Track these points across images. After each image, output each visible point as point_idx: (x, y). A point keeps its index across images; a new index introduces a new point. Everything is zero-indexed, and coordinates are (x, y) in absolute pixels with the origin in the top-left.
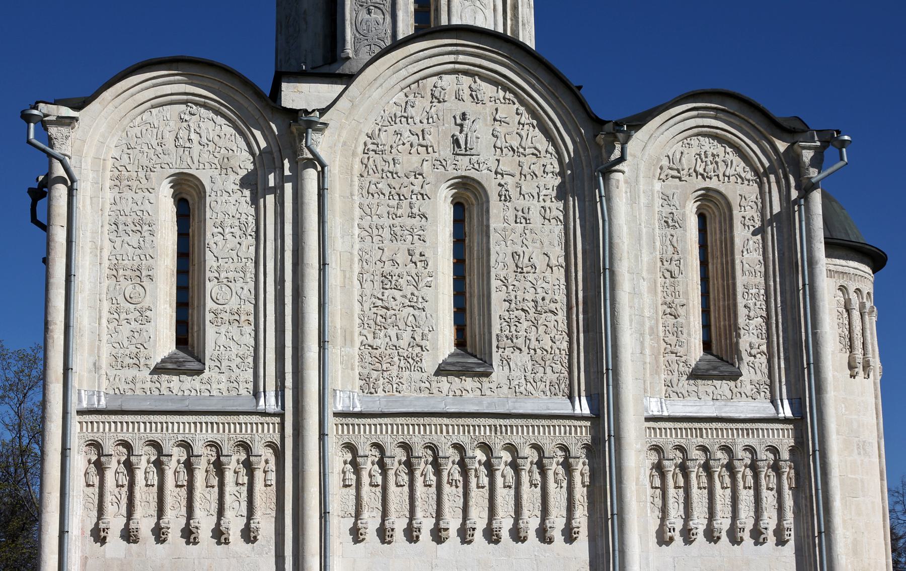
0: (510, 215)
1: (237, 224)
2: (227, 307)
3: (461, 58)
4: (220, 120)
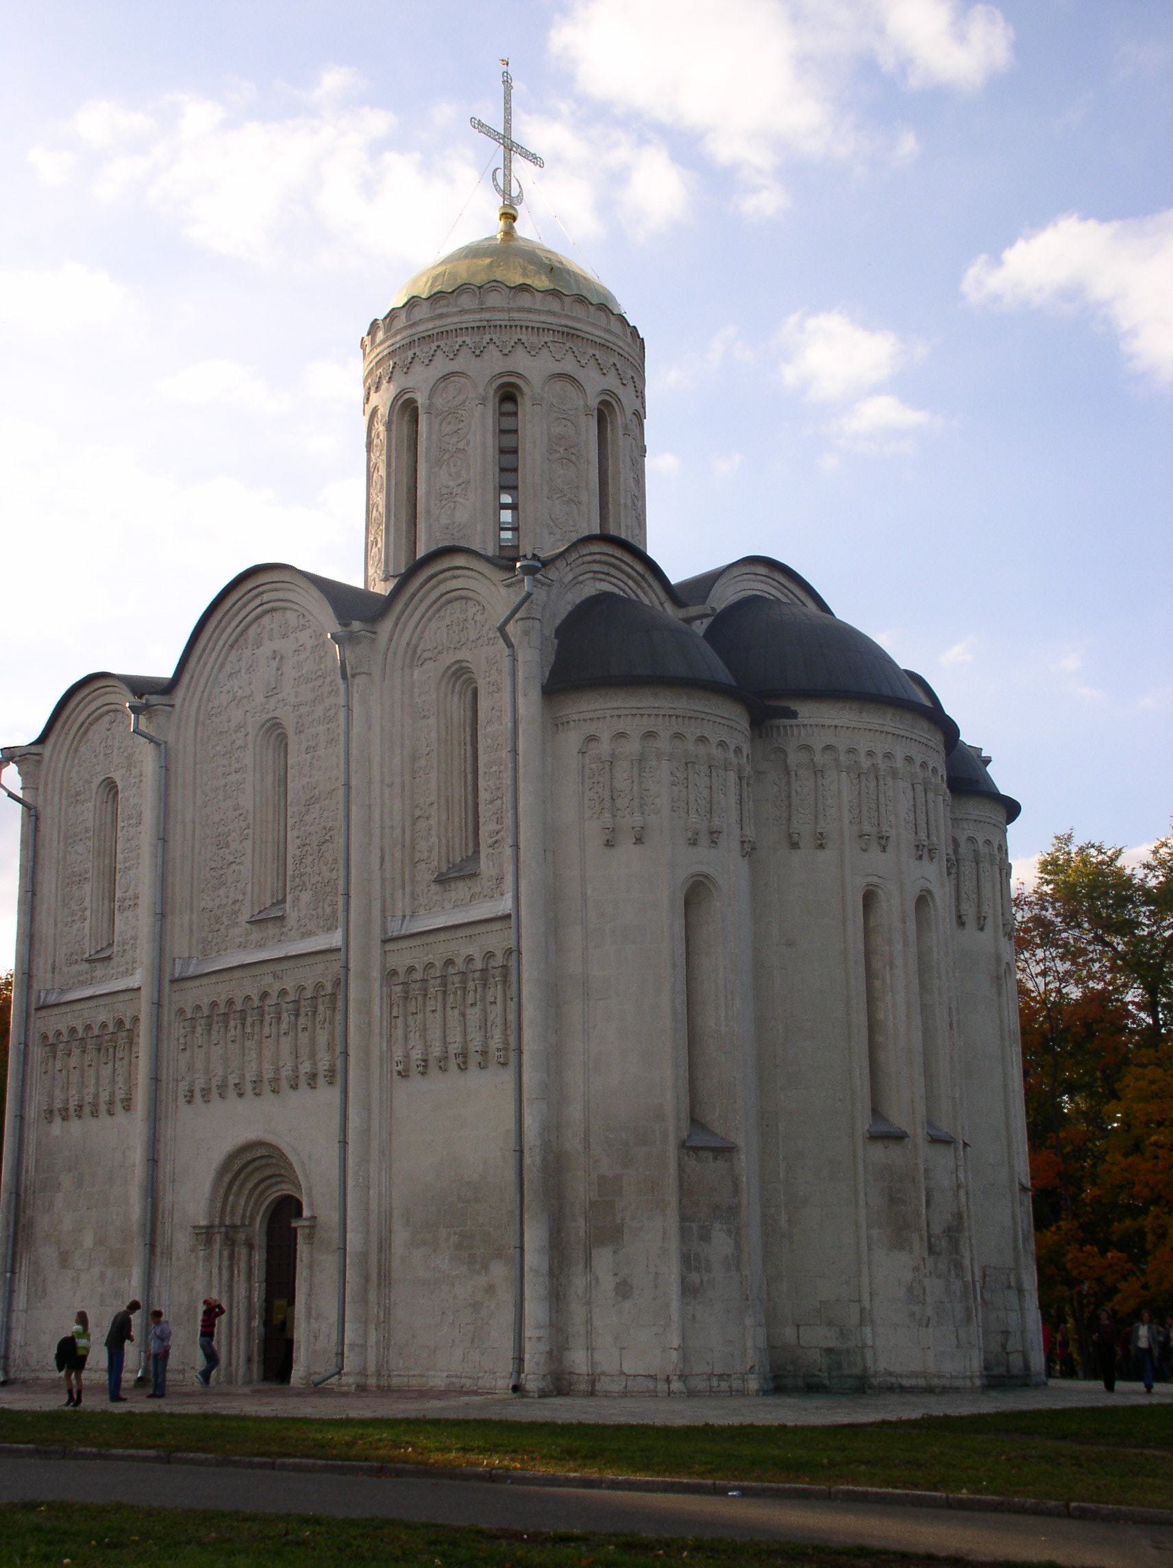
0: (304, 746)
3: (266, 597)
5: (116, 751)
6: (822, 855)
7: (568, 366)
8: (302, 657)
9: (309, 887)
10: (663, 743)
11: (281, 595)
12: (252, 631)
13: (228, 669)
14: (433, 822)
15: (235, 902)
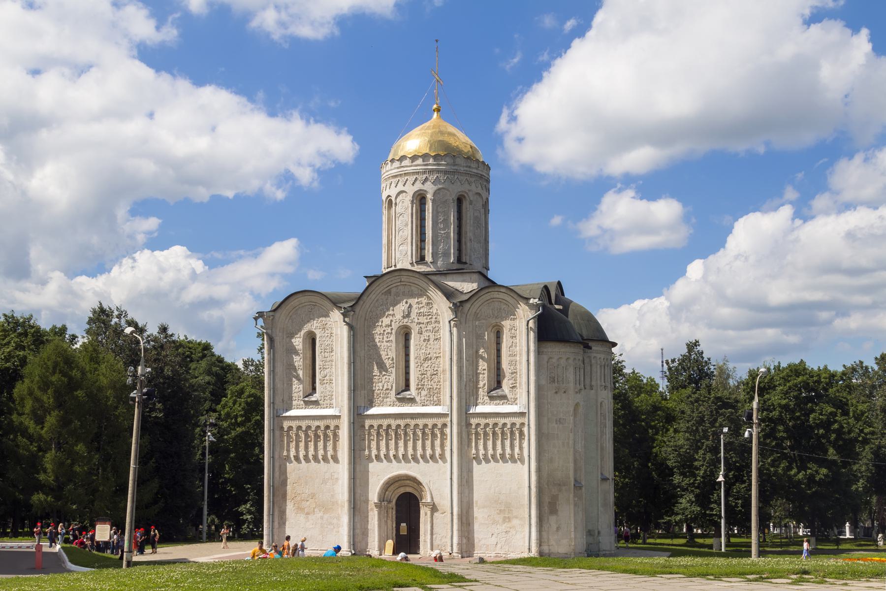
0: (422, 339)
6: (593, 391)
7: (479, 190)
8: (421, 305)
10: (571, 361)
14: (486, 375)
15: (387, 389)
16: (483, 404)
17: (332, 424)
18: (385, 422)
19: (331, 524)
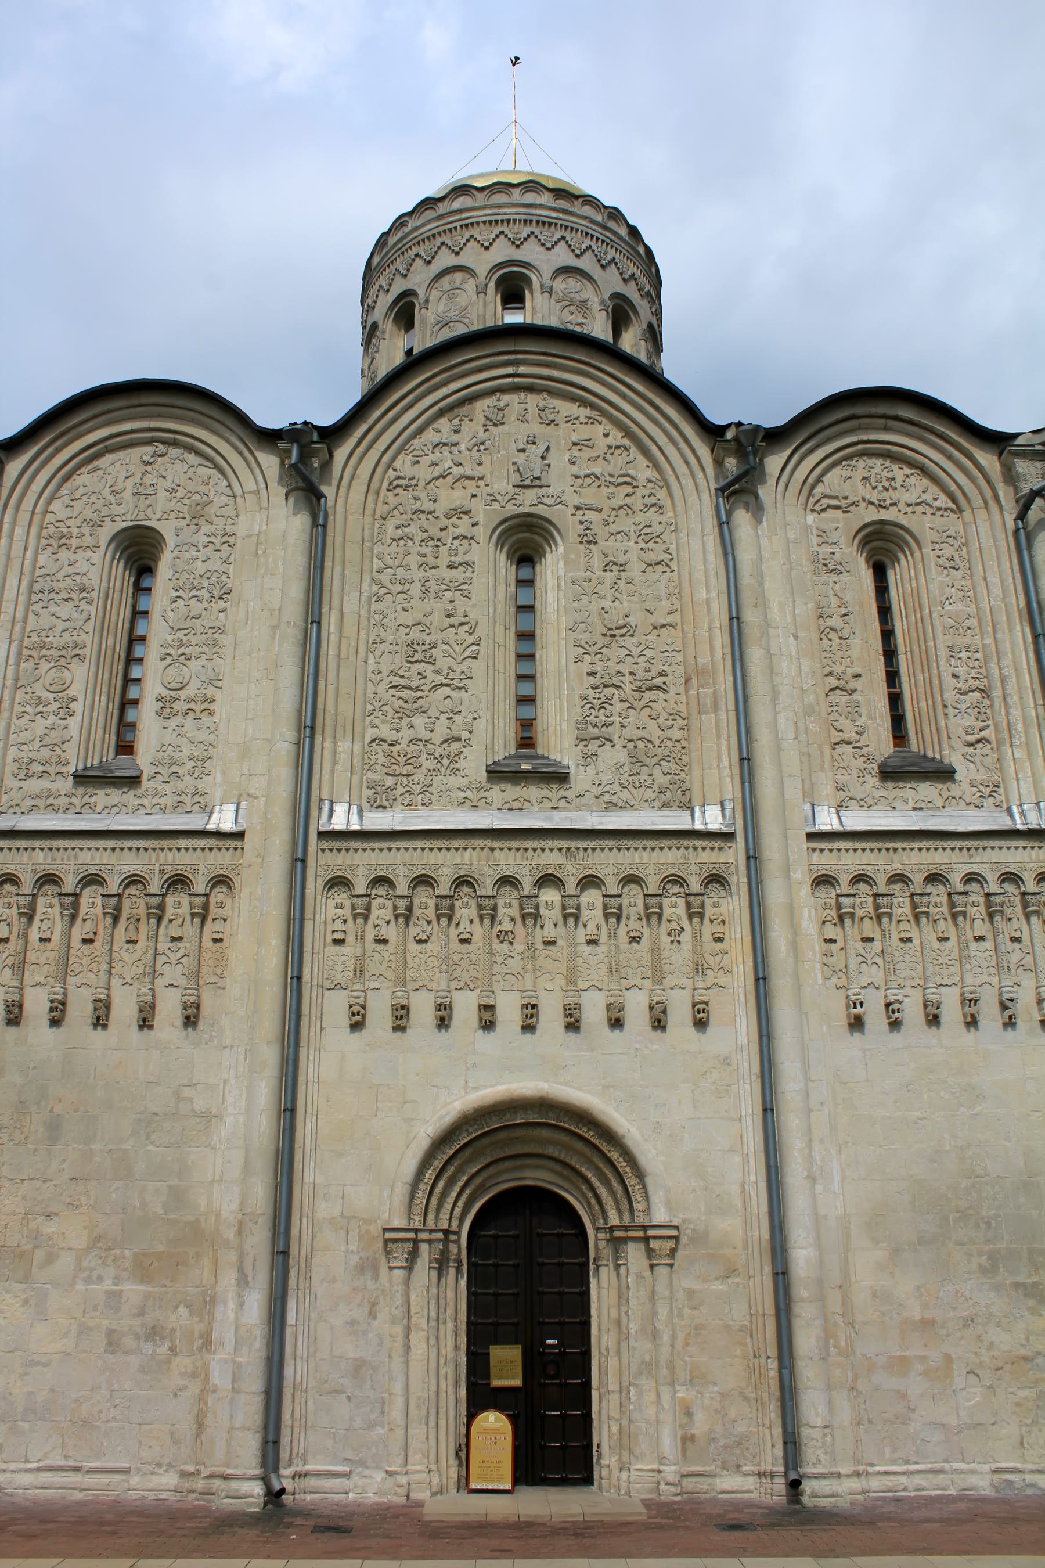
0: (597, 562)
1: (206, 585)
2: (183, 694)
3: (522, 369)
4: (192, 458)
5: (162, 495)
9: (619, 743)
11: (555, 373)
12: (483, 405)
13: (430, 436)
16: (865, 804)
17: (201, 863)
18: (446, 862)
19: (154, 1333)
